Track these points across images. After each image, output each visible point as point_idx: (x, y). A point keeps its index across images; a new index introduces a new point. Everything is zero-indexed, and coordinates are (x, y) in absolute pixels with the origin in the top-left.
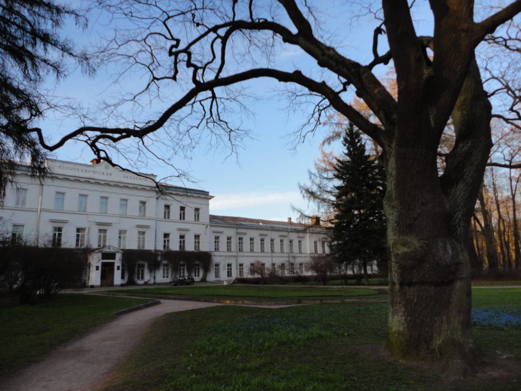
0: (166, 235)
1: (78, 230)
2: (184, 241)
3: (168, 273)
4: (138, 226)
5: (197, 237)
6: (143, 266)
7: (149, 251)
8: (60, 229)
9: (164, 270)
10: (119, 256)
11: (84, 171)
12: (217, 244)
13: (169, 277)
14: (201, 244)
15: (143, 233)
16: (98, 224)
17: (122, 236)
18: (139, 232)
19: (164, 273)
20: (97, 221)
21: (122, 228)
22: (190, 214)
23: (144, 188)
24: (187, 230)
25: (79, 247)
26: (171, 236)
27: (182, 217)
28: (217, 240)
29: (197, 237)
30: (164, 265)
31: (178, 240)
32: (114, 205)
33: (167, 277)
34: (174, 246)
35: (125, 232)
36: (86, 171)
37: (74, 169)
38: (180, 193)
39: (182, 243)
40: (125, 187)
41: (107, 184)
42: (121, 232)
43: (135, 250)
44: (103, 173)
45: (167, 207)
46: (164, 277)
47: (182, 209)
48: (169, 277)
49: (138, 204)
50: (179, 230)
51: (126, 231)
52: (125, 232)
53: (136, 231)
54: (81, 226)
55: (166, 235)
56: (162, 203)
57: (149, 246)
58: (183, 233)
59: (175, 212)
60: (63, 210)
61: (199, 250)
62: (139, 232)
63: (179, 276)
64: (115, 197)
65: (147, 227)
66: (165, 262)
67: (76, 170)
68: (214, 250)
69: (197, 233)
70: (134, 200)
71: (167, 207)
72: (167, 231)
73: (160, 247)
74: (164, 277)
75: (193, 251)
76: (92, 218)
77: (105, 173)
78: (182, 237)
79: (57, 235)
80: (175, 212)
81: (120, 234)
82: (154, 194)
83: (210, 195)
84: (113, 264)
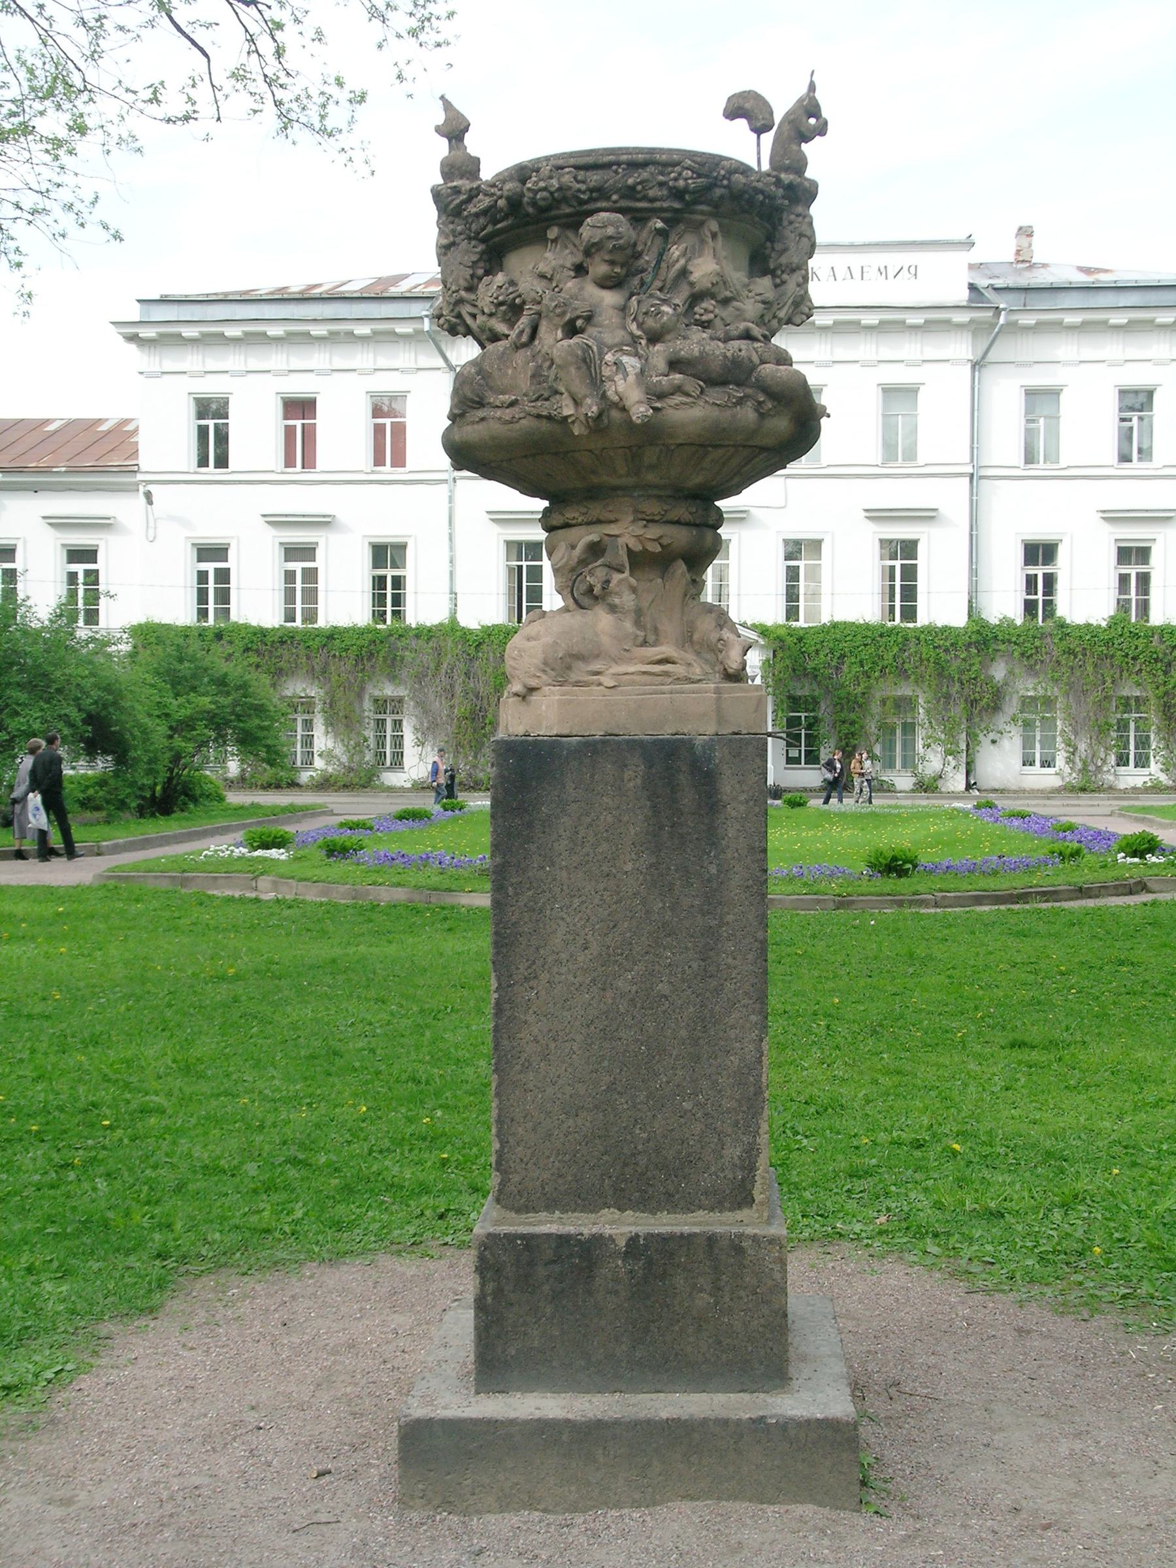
0: (1039, 552)
2: (1144, 580)
3: (1048, 742)
4: (877, 516)
6: (904, 705)
7: (938, 635)
9: (1028, 725)
13: (1060, 760)
14: (1061, 586)
18: (509, 544)
19: (1028, 743)
25: (298, 623)
26: (1062, 553)
30: (1028, 703)
33: (1047, 763)
35: (815, 546)
38: (1070, 319)
40: (883, 328)
42: (794, 549)
43: (867, 626)
45: (1041, 399)
46: (1028, 762)
48: (1060, 760)
50: (1112, 518)
52: (815, 546)
56: (1005, 394)
57: (941, 606)
58: (1134, 534)
59: (1089, 427)
63: (1112, 759)
65: (927, 516)
66: (1027, 687)
73: (1005, 604)
74: (1028, 762)
79: (81, 578)
82: (961, 348)
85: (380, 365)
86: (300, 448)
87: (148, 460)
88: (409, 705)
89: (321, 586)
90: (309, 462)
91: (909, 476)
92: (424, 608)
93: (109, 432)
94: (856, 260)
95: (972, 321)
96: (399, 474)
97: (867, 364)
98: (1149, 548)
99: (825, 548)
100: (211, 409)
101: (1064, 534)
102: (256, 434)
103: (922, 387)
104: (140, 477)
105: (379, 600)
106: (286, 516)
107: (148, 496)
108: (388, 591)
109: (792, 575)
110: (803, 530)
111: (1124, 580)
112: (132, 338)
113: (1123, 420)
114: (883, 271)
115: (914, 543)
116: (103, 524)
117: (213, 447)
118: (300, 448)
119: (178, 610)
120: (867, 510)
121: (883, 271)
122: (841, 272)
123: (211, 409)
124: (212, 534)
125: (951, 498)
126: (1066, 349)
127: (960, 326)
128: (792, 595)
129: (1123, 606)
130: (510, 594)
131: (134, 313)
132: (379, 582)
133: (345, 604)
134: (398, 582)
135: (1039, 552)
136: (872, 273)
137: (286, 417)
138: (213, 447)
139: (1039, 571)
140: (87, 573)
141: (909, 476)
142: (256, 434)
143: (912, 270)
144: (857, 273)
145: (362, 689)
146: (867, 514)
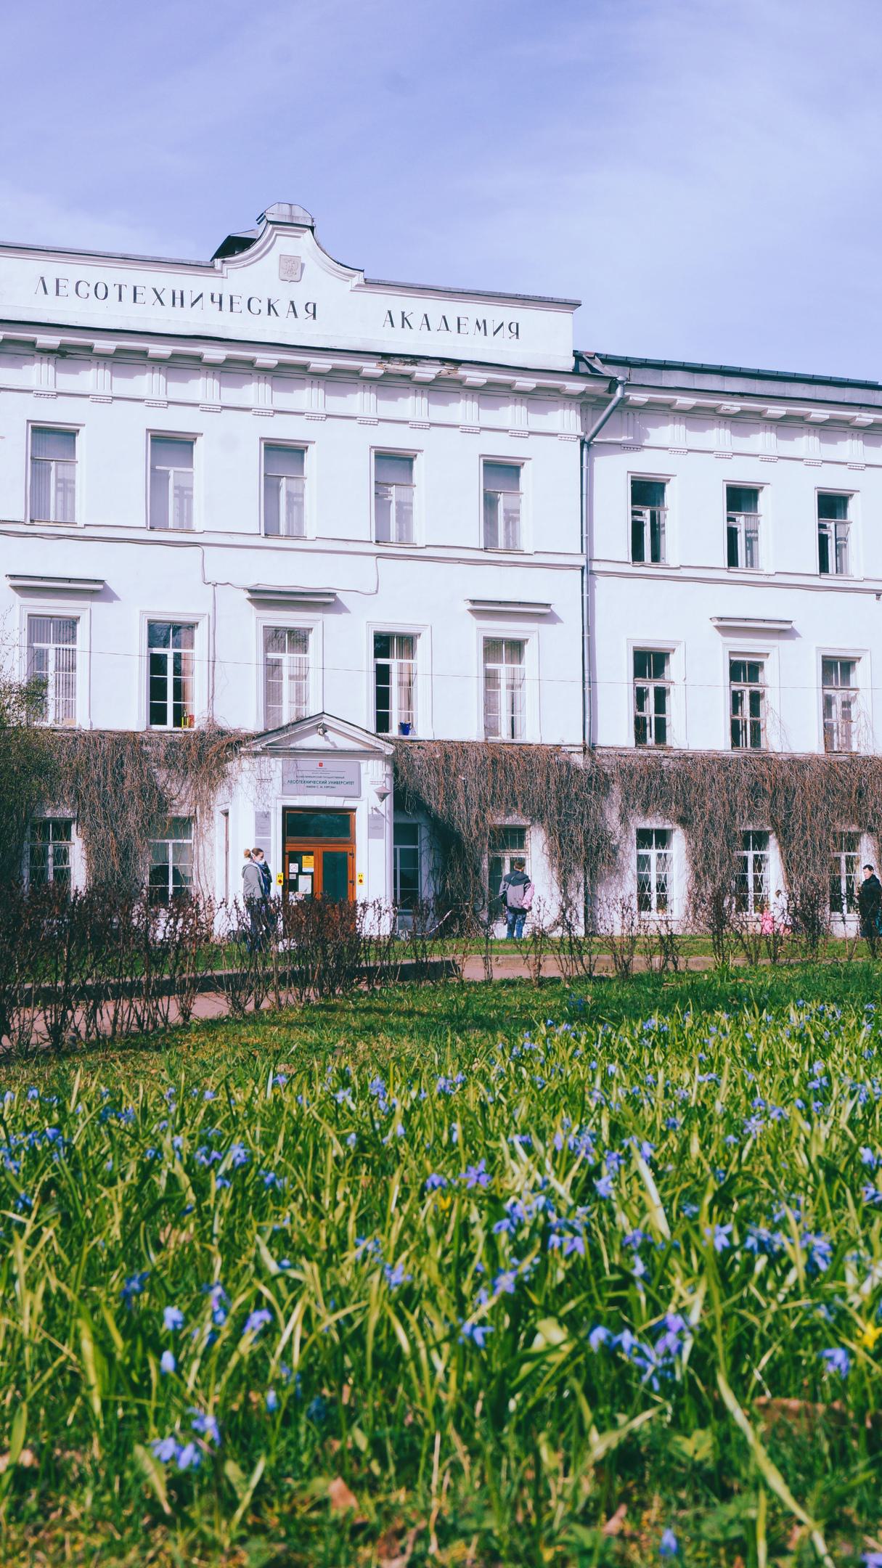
0: (649, 662)
4: (484, 609)
11: (167, 297)
16: (263, 598)
17: (394, 663)
20: (250, 584)
23: (500, 386)
29: (837, 668)
32: (336, 487)
34: (699, 725)
35: (407, 643)
36: (178, 299)
37: (113, 292)
39: (650, 702)
41: (291, 369)
42: (383, 644)
44: (270, 306)
47: (741, 498)
50: (728, 627)
51: (192, 627)
52: (407, 643)
54: (170, 610)
55: (649, 662)
56: (614, 474)
60: (72, 524)
64: (345, 438)
70: (449, 446)
71: (647, 492)
72: (652, 639)
76: (223, 564)
77: (283, 307)
78: (744, 670)
80: (693, 523)
81: (378, 653)
82: (567, 420)
85: (172, 397)
88: (773, 841)
94: (454, 309)
95: (583, 393)
97: (467, 430)
98: (761, 664)
99: (420, 644)
101: (678, 643)
103: (311, 447)
106: (500, 603)
109: (382, 674)
110: (394, 623)
113: (634, 513)
114: (482, 325)
120: (473, 602)
121: (482, 325)
122: (436, 322)
126: (667, 433)
127: (570, 397)
128: (382, 698)
130: (596, 702)
136: (469, 326)
139: (650, 686)
141: (516, 564)
143: (514, 328)
145: (683, 821)
146: (717, 623)
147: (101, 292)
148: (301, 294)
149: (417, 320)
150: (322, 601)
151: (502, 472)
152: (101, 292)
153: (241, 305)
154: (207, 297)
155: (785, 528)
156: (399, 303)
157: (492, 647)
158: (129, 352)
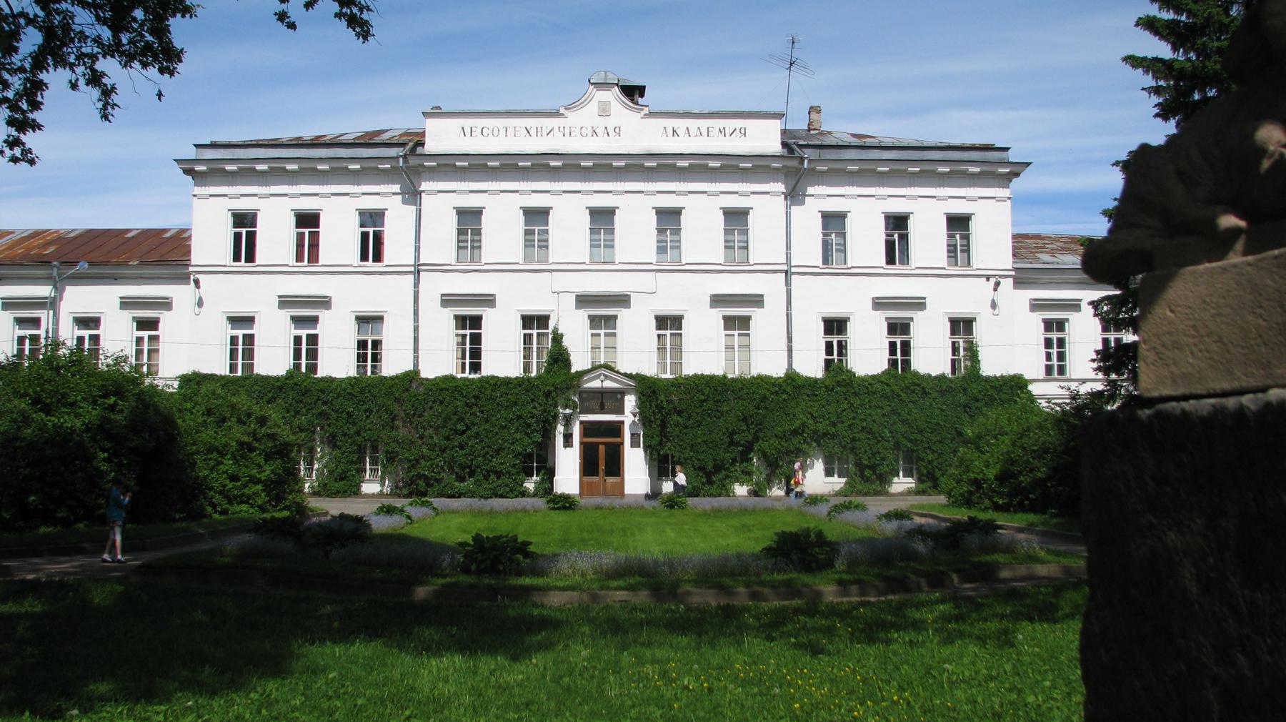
0: (835, 326)
1: (528, 321)
5: (962, 326)
8: (476, 322)
10: (630, 402)
11: (533, 132)
12: (1054, 351)
15: (744, 322)
21: (669, 309)
22: (928, 239)
24: (919, 304)
27: (897, 250)
28: (1054, 336)
29: (962, 326)
31: (883, 340)
45: (834, 221)
47: (898, 223)
49: (518, 223)
53: (879, 322)
59: (866, 239)
61: (249, 367)
62: (725, 318)
65: (756, 301)
67: (510, 131)
68: (1042, 375)
69: (962, 310)
71: (834, 221)
72: (836, 311)
75: (449, 379)
76: (561, 281)
77: (600, 131)
78: (898, 327)
83: (1012, 156)
84: (616, 429)
86: (308, 249)
87: (198, 256)
89: (483, 346)
90: (314, 258)
91: (743, 271)
92: (394, 364)
93: (171, 237)
96: (378, 267)
100: (244, 220)
102: (276, 237)
104: (191, 269)
105: (362, 358)
107: (197, 282)
108: (369, 351)
111: (892, 346)
112: (188, 172)
114: (722, 131)
115: (748, 319)
116: (165, 304)
117: (245, 248)
118: (308, 249)
119: (217, 365)
122: (693, 131)
123: (244, 220)
124: (242, 309)
125: (771, 287)
129: (893, 363)
131: (192, 153)
132: (362, 345)
133: (337, 362)
134: (376, 344)
135: (835, 326)
137: (298, 226)
138: (245, 248)
140: (151, 337)
141: (743, 271)
142: (276, 237)
144: (705, 133)
147: (496, 132)
148: (611, 123)
149: (681, 131)
150: (622, 300)
151: (736, 218)
152: (496, 132)
153: (576, 132)
154: (556, 129)
155: (928, 239)
156: (671, 123)
157: (729, 322)
158: (509, 166)
